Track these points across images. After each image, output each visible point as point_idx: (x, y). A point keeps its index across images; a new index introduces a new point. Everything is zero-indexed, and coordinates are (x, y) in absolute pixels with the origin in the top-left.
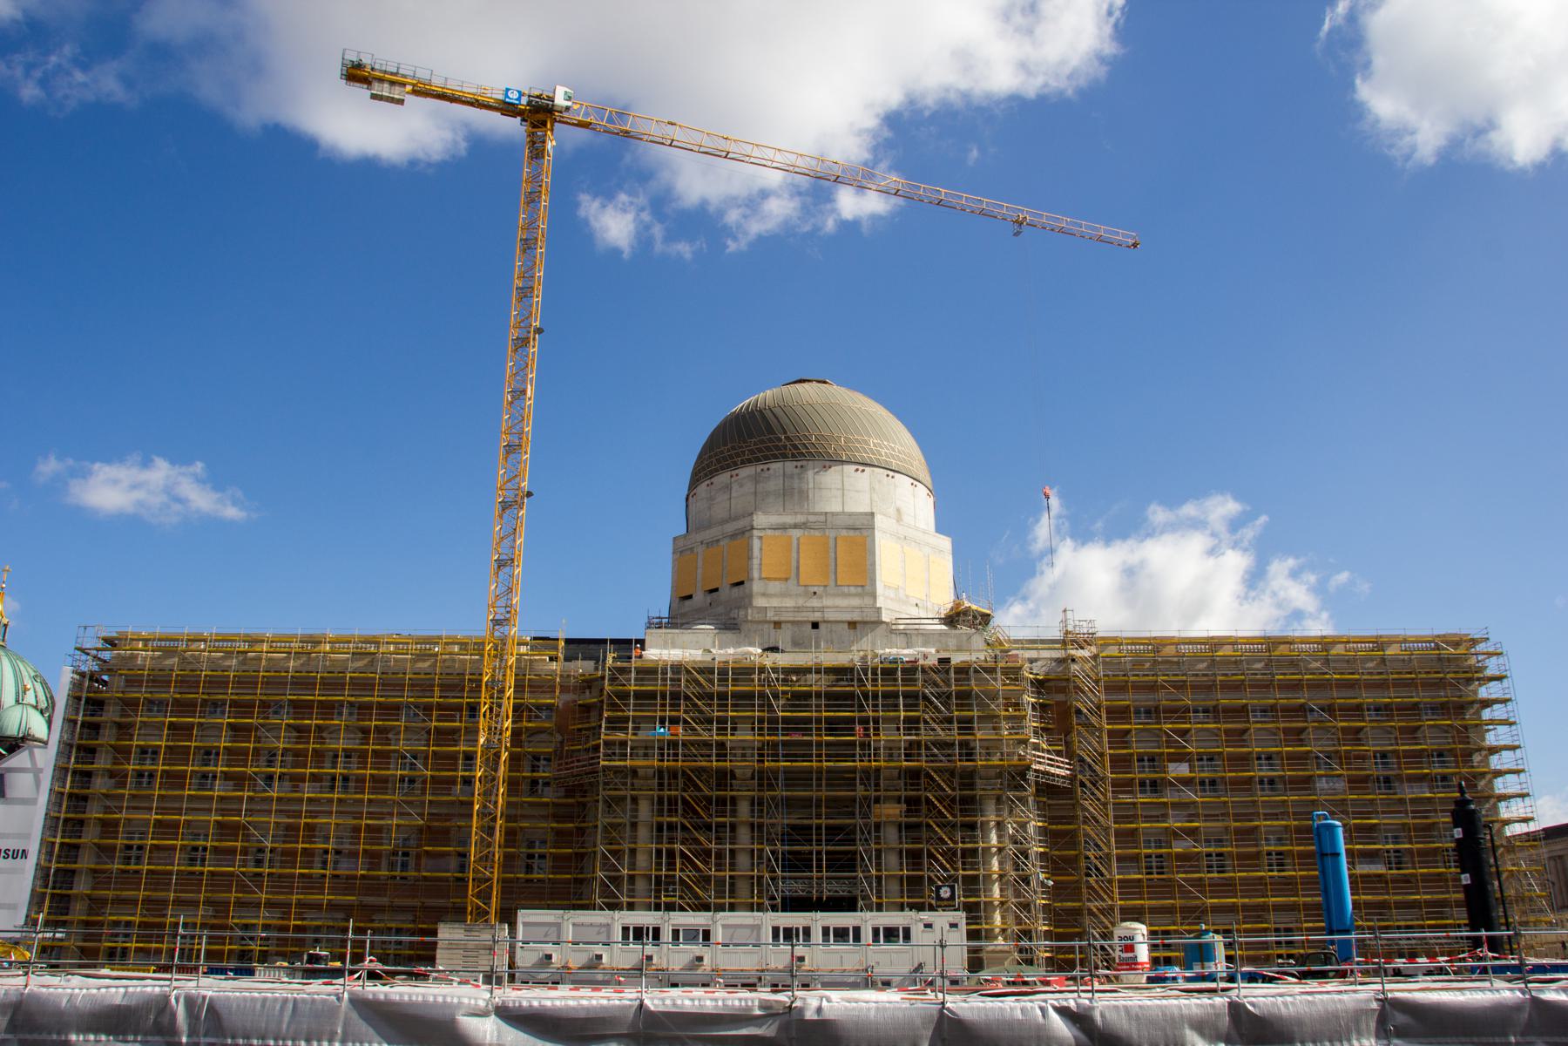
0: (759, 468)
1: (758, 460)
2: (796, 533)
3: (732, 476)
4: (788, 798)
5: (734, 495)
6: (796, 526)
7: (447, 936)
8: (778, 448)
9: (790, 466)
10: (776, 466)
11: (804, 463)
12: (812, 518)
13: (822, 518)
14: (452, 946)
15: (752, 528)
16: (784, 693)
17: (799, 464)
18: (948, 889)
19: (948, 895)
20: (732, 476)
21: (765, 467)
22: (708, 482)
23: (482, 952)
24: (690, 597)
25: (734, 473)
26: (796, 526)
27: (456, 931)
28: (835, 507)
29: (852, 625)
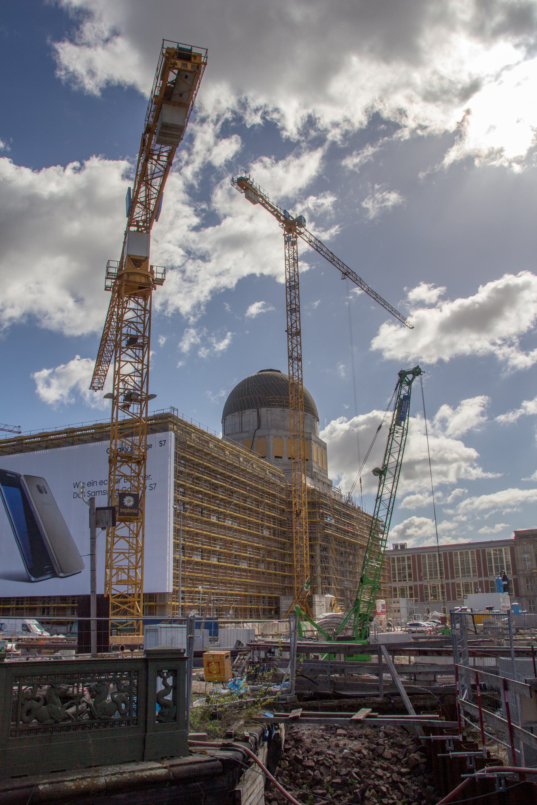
10: (309, 414)
15: (311, 439)
21: (307, 413)
24: (281, 457)
29: (328, 485)
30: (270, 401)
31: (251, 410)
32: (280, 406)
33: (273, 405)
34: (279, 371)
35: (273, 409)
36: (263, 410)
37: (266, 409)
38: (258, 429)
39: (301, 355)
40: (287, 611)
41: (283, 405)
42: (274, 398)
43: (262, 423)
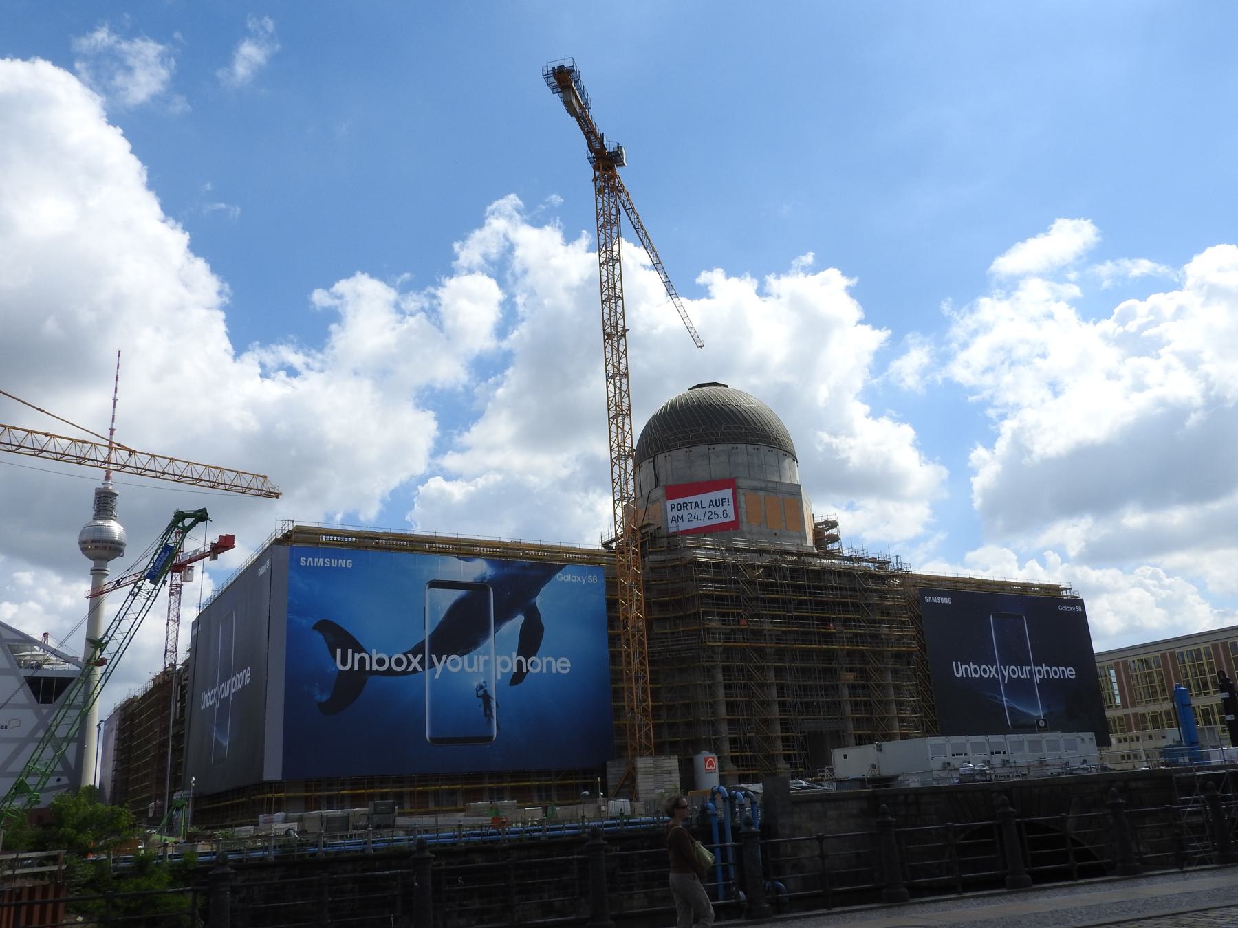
0: (730, 446)
1: (728, 442)
2: (762, 493)
3: (709, 449)
4: (802, 668)
5: (712, 461)
6: (761, 489)
7: (643, 766)
8: (741, 434)
9: (750, 447)
10: (741, 447)
11: (759, 447)
12: (769, 485)
13: (774, 485)
14: (647, 772)
16: (794, 600)
17: (756, 447)
18: (1041, 725)
19: (1043, 724)
20: (709, 449)
21: (735, 446)
22: (687, 449)
23: (665, 775)
25: (711, 447)
26: (761, 489)
27: (649, 762)
28: (788, 481)
30: (669, 441)
31: (647, 461)
32: (683, 444)
33: (673, 446)
34: (715, 384)
35: (674, 453)
36: (661, 458)
37: (663, 455)
38: (656, 487)
39: (627, 368)
40: (617, 786)
41: (689, 443)
42: (675, 434)
43: (661, 479)
